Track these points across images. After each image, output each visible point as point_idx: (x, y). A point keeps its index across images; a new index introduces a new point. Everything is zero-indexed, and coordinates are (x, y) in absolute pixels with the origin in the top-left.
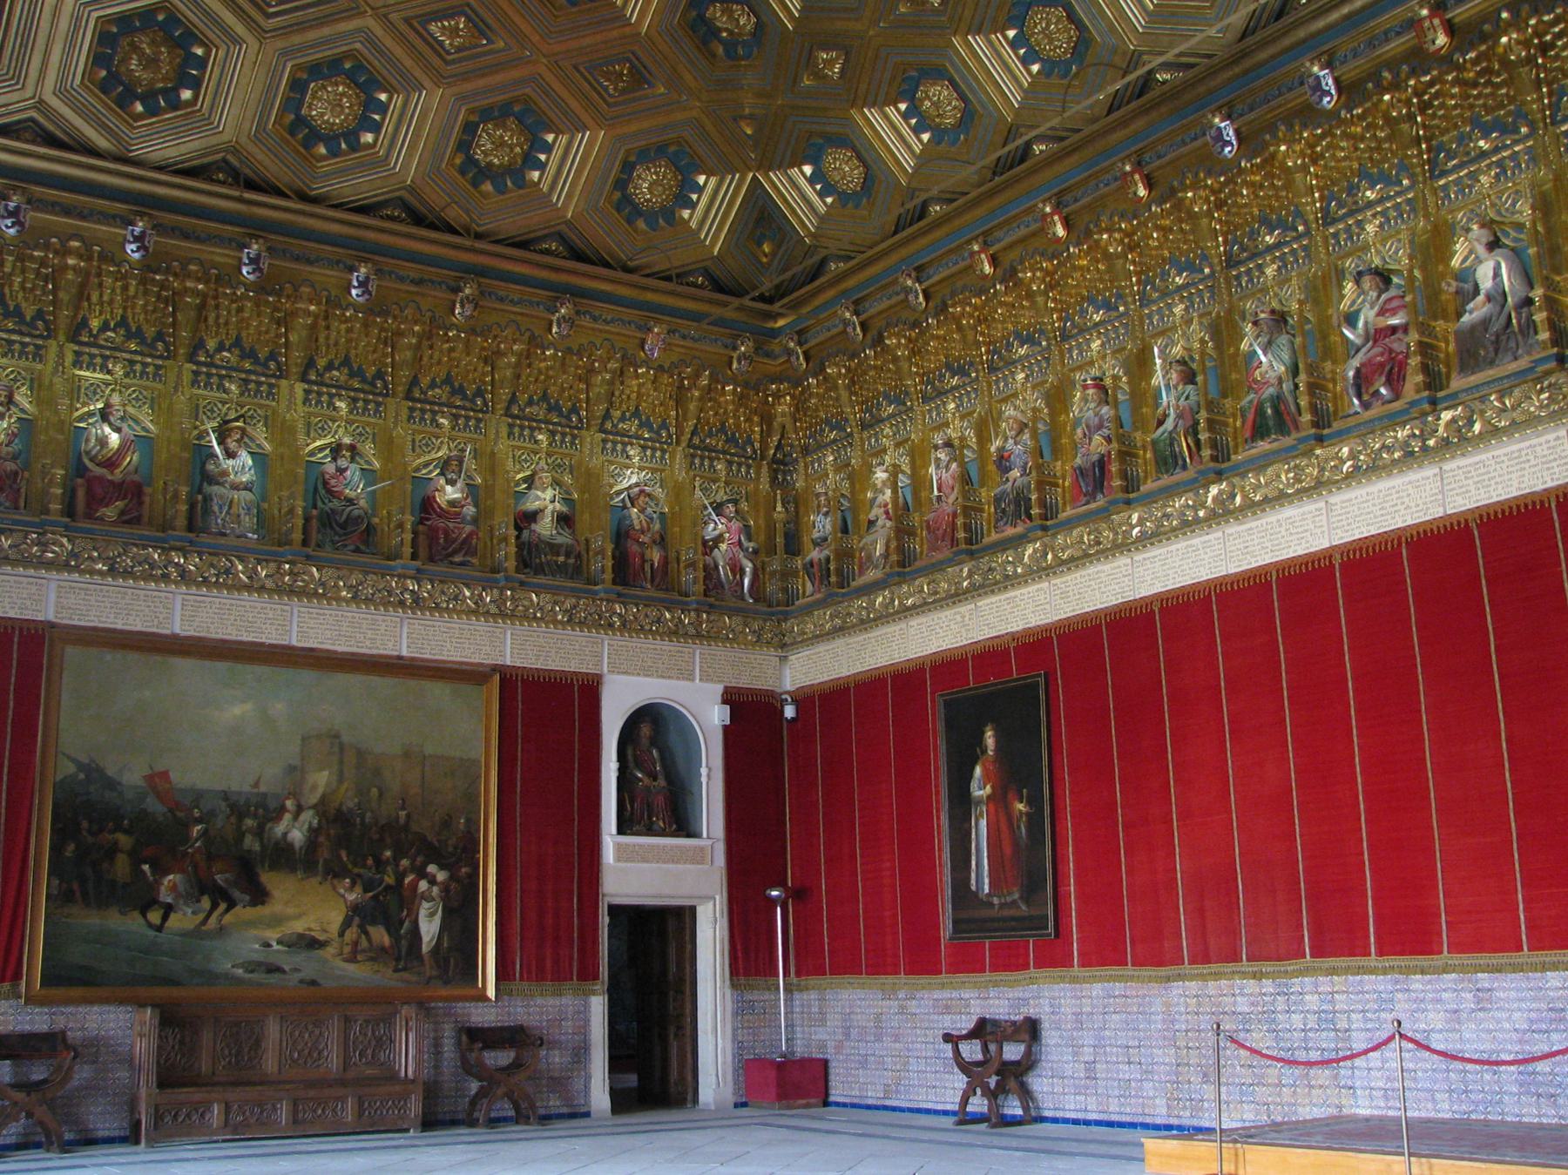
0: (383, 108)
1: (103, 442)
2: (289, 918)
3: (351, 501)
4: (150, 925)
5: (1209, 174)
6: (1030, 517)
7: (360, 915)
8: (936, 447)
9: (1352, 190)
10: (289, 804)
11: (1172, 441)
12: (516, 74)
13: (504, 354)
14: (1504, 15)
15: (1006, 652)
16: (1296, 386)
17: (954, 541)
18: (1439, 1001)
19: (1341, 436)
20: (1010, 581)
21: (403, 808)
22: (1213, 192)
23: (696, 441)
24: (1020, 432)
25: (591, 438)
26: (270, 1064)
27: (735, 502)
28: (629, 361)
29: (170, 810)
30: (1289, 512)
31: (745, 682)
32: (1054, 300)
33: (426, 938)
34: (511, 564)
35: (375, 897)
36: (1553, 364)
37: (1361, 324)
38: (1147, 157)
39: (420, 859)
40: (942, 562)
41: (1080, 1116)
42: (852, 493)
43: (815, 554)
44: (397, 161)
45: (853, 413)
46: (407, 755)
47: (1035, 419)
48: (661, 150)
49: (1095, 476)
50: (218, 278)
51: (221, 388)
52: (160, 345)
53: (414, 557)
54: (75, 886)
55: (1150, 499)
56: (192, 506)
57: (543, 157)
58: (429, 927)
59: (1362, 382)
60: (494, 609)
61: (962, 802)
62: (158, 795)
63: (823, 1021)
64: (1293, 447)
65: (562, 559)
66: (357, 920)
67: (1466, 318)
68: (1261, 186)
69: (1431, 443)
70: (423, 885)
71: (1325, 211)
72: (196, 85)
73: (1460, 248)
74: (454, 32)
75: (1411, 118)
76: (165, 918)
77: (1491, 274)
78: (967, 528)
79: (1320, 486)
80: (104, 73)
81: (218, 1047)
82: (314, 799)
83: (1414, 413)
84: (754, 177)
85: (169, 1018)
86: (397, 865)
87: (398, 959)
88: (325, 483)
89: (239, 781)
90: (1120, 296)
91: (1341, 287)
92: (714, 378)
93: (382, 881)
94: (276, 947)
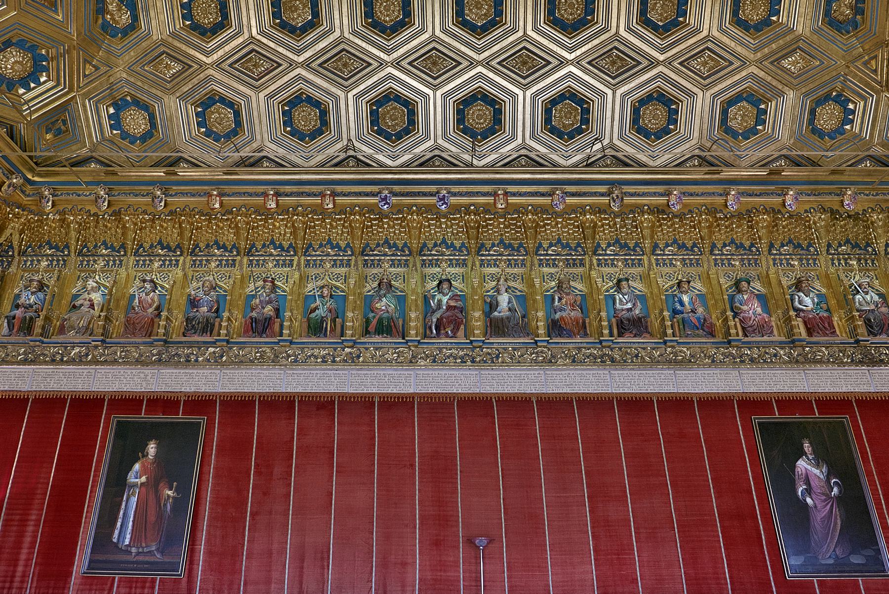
15: (64, 400)
61: (117, 484)
67: (496, 313)
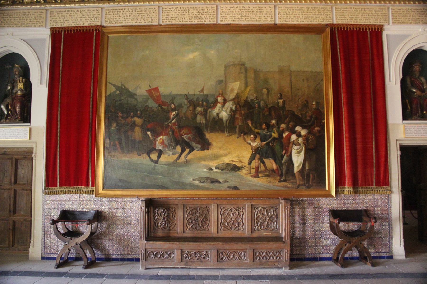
2: (221, 156)
4: (152, 160)
7: (259, 154)
10: (219, 99)
21: (281, 98)
29: (160, 106)
35: (268, 144)
39: (291, 124)
46: (281, 71)
54: (117, 142)
58: (298, 159)
62: (153, 99)
70: (294, 137)
76: (159, 157)
81: (186, 220)
82: (232, 96)
86: (279, 128)
87: (281, 175)
89: (193, 90)
93: (271, 135)
94: (215, 170)
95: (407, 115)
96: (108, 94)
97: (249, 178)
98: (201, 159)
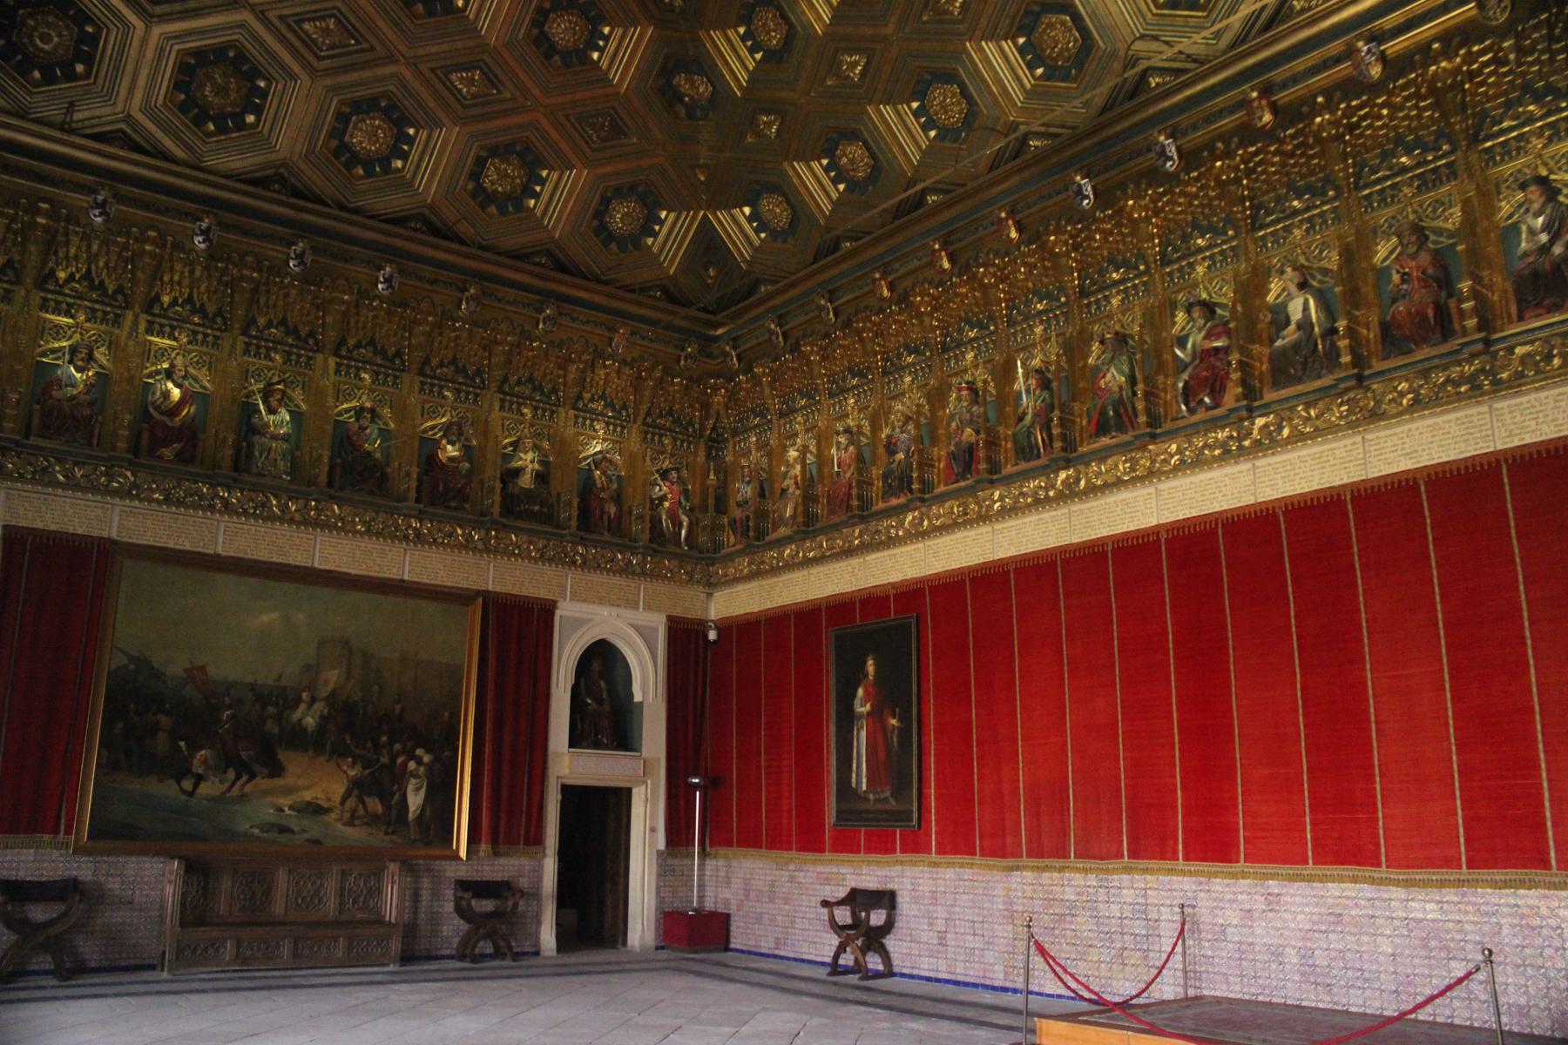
0: (411, 141)
1: (166, 394)
3: (369, 453)
4: (183, 791)
5: (1068, 222)
6: (911, 491)
7: (358, 788)
8: (838, 433)
9: (1186, 238)
10: (304, 695)
11: (1029, 434)
12: (519, 119)
13: (500, 344)
14: (1320, 99)
16: (1135, 394)
17: (849, 508)
18: (1235, 901)
19: (1170, 435)
20: (891, 542)
22: (1072, 237)
23: (649, 420)
24: (905, 423)
25: (565, 415)
26: (278, 909)
27: (678, 470)
28: (599, 355)
30: (1124, 495)
31: (679, 612)
32: (938, 320)
33: (412, 808)
34: (496, 510)
35: (372, 774)
36: (1352, 383)
37: (1189, 345)
38: (1019, 207)
40: (837, 525)
41: (932, 975)
42: (770, 465)
43: (738, 513)
44: (421, 184)
45: (775, 404)
47: (919, 413)
48: (632, 189)
49: (965, 460)
50: (270, 269)
51: (268, 357)
52: (219, 320)
53: (417, 501)
55: (1008, 480)
56: (238, 451)
57: (538, 189)
58: (415, 800)
59: (1188, 394)
60: (480, 546)
61: (847, 718)
63: (729, 883)
64: (1129, 443)
65: (537, 508)
66: (356, 792)
67: (1279, 343)
68: (1111, 233)
69: (1247, 443)
70: (412, 765)
71: (1163, 254)
72: (258, 111)
73: (1275, 287)
74: (471, 81)
75: (1238, 181)
76: (196, 786)
77: (1300, 308)
78: (860, 497)
79: (1151, 475)
80: (183, 97)
82: (324, 692)
83: (1234, 418)
84: (705, 216)
85: (193, 868)
87: (388, 824)
88: (349, 438)
90: (991, 318)
91: (1173, 316)
92: (666, 372)
93: (378, 760)
94: (287, 811)
95: (574, 742)
96: (113, 667)
97: (339, 826)
98: (267, 792)
